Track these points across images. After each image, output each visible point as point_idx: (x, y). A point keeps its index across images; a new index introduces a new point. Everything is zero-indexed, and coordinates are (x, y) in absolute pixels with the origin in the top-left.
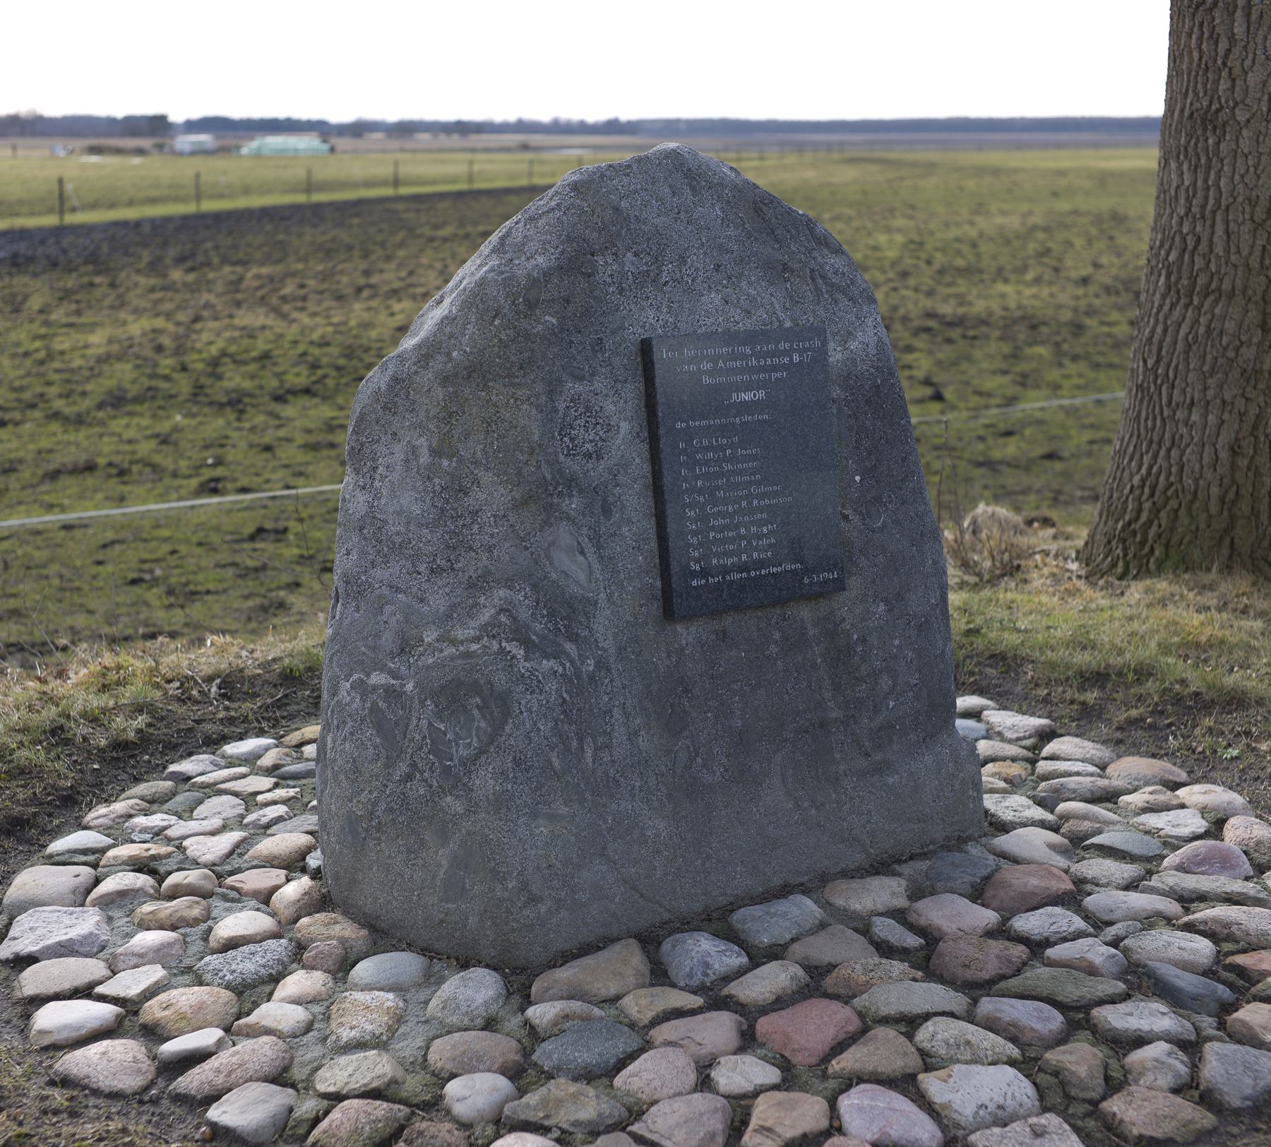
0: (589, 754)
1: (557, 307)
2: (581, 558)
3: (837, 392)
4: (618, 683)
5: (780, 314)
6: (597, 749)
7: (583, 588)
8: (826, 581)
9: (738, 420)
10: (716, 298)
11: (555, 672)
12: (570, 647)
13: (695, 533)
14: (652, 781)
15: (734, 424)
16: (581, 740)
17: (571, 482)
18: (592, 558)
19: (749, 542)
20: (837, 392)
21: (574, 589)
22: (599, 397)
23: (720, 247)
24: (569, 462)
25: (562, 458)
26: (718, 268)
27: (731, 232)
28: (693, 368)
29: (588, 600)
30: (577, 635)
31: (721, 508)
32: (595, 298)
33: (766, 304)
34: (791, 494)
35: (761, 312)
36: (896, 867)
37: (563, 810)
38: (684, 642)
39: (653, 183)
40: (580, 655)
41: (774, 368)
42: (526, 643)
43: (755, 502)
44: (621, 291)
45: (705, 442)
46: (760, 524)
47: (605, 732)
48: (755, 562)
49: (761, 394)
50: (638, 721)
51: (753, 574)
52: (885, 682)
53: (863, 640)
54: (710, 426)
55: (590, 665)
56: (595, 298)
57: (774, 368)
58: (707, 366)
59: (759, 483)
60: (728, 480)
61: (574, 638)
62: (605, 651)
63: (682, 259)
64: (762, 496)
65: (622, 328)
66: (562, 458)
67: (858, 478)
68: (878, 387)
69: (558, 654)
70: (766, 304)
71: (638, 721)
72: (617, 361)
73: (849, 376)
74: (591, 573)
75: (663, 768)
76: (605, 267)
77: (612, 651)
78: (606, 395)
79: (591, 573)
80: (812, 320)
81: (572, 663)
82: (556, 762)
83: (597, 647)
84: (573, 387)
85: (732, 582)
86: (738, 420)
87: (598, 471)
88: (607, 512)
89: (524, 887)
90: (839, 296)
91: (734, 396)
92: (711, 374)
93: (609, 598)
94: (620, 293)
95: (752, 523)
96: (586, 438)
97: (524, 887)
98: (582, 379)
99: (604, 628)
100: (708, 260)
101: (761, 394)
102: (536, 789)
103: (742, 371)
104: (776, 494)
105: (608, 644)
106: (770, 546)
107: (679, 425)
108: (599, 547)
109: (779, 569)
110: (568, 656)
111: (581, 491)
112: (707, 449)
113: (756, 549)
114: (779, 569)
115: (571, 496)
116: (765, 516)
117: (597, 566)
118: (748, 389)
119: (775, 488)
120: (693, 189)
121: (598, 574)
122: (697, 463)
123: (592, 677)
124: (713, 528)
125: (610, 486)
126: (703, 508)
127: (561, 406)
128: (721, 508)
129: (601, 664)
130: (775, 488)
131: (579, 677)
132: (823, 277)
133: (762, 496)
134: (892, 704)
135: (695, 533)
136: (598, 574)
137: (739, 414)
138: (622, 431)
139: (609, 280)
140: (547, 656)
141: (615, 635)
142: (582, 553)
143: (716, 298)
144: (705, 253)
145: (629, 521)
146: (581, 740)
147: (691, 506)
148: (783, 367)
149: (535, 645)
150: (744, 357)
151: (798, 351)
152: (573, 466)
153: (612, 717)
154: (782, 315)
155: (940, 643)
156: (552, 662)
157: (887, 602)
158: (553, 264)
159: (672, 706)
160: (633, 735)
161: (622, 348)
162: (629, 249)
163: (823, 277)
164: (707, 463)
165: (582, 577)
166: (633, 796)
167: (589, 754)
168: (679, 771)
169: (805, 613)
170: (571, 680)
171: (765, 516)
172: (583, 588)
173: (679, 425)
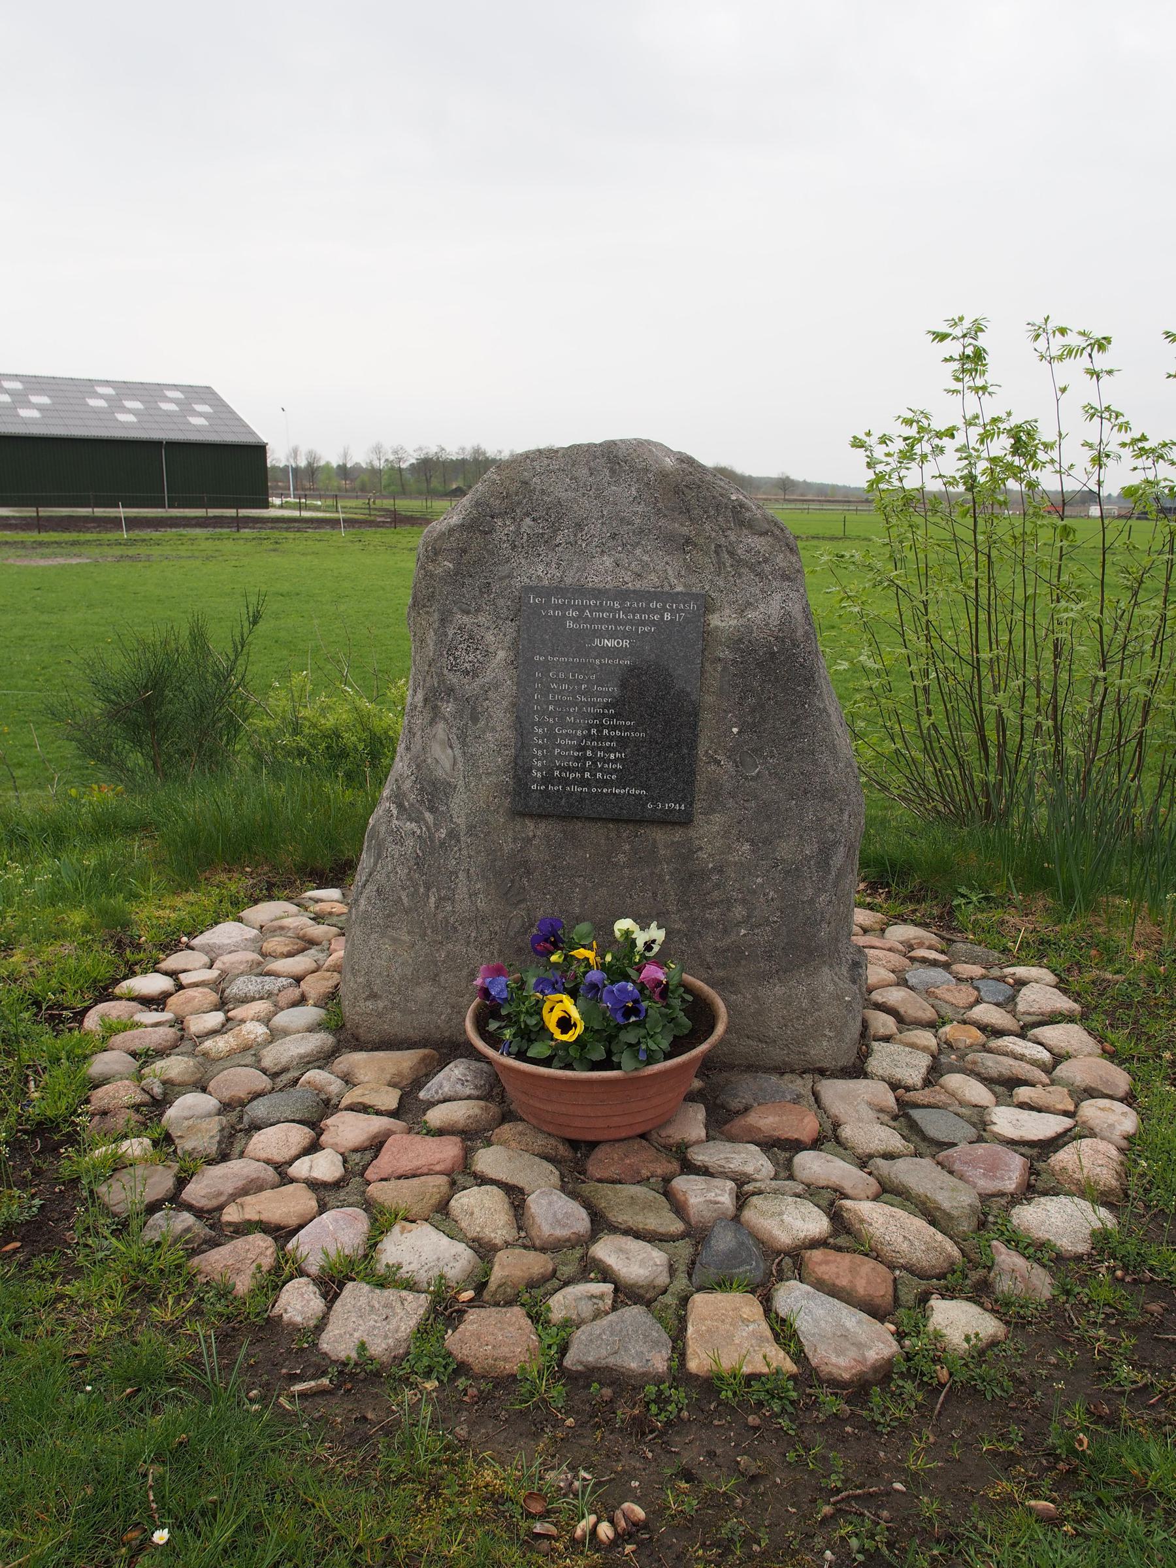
0: (432, 900)
1: (454, 555)
2: (450, 751)
3: (725, 653)
4: (465, 852)
5: (672, 580)
6: (441, 899)
7: (447, 774)
8: (671, 811)
9: (597, 662)
10: (608, 561)
11: (414, 833)
12: (428, 816)
13: (540, 747)
14: (486, 936)
15: (593, 664)
16: (428, 889)
17: (451, 691)
18: (458, 752)
19: (594, 763)
20: (725, 653)
21: (439, 773)
22: (482, 629)
23: (622, 520)
24: (450, 676)
25: (445, 672)
26: (614, 536)
27: (640, 509)
28: (558, 613)
29: (449, 784)
30: (437, 808)
31: (570, 731)
32: (488, 551)
33: (664, 571)
34: (645, 731)
35: (653, 576)
36: (422, 1095)
37: (406, 938)
38: (531, 834)
39: (573, 465)
40: (435, 824)
41: (642, 623)
42: (400, 806)
43: (606, 732)
44: (514, 547)
45: (562, 675)
46: (609, 750)
47: (449, 888)
48: (597, 781)
49: (626, 643)
50: (478, 886)
51: (594, 790)
52: (739, 912)
53: (720, 870)
54: (567, 663)
55: (443, 833)
56: (488, 551)
57: (642, 623)
58: (572, 613)
59: (611, 717)
60: (580, 709)
61: (432, 809)
62: (458, 825)
63: (579, 526)
64: (614, 728)
65: (510, 576)
66: (445, 672)
67: (735, 730)
68: (773, 654)
69: (419, 820)
70: (664, 571)
71: (478, 886)
72: (501, 602)
73: (740, 640)
74: (455, 764)
75: (497, 928)
76: (504, 529)
77: (463, 827)
78: (488, 628)
79: (455, 764)
80: (707, 588)
81: (428, 828)
82: (405, 900)
83: (451, 821)
84: (461, 619)
85: (572, 793)
86: (597, 662)
87: (472, 687)
88: (475, 719)
89: (369, 984)
90: (745, 570)
91: (597, 642)
92: (575, 620)
93: (467, 785)
94: (512, 549)
95: (600, 749)
96: (467, 659)
97: (369, 984)
98: (468, 613)
99: (459, 808)
100: (604, 530)
101: (626, 643)
102: (388, 916)
103: (608, 621)
104: (628, 728)
105: (461, 821)
106: (615, 770)
107: (537, 658)
108: (464, 744)
109: (622, 791)
110: (426, 823)
111: (456, 699)
112: (563, 681)
113: (601, 770)
114: (622, 791)
115: (448, 702)
116: (614, 744)
117: (460, 759)
118: (611, 636)
119: (628, 723)
120: (613, 472)
121: (460, 765)
122: (550, 690)
123: (442, 844)
124: (559, 746)
125: (481, 699)
126: (551, 729)
127: (451, 632)
128: (570, 731)
129: (452, 834)
130: (628, 723)
131: (432, 841)
132: (732, 554)
133: (614, 728)
134: (743, 932)
135: (540, 747)
136: (460, 765)
137: (599, 656)
138: (498, 658)
139: (505, 538)
140: (411, 820)
141: (468, 815)
142: (451, 747)
143: (608, 561)
144: (603, 524)
145: (494, 729)
146: (428, 889)
147: (539, 725)
148: (653, 623)
149: (406, 810)
150: (611, 610)
151: (671, 611)
152: (453, 679)
153: (457, 877)
154: (674, 581)
155: (810, 892)
156: (414, 824)
157: (752, 842)
158: (459, 522)
159: (512, 881)
160: (473, 895)
161: (506, 593)
162: (528, 514)
163: (732, 554)
164: (560, 692)
165: (448, 765)
166: (468, 943)
167: (432, 900)
168: (512, 934)
169: (660, 836)
170: (425, 842)
171: (614, 744)
172: (447, 774)
173: (537, 658)
